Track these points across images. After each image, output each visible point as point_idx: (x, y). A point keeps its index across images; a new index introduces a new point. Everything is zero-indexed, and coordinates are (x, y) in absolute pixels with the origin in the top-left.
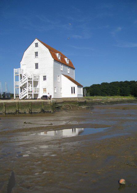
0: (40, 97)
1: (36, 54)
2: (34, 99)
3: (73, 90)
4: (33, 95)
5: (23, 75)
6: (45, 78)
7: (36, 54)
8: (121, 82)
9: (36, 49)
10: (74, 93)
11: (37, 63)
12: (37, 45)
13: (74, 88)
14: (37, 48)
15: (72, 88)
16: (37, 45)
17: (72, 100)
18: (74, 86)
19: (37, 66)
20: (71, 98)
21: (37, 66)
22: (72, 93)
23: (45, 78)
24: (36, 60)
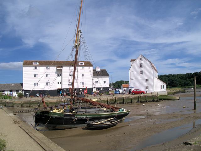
1: (141, 65)
3: (162, 87)
6: (147, 80)
7: (141, 65)
9: (141, 62)
12: (141, 59)
13: (163, 85)
15: (162, 85)
16: (141, 59)
18: (164, 84)
19: (141, 72)
21: (141, 72)
22: (162, 89)
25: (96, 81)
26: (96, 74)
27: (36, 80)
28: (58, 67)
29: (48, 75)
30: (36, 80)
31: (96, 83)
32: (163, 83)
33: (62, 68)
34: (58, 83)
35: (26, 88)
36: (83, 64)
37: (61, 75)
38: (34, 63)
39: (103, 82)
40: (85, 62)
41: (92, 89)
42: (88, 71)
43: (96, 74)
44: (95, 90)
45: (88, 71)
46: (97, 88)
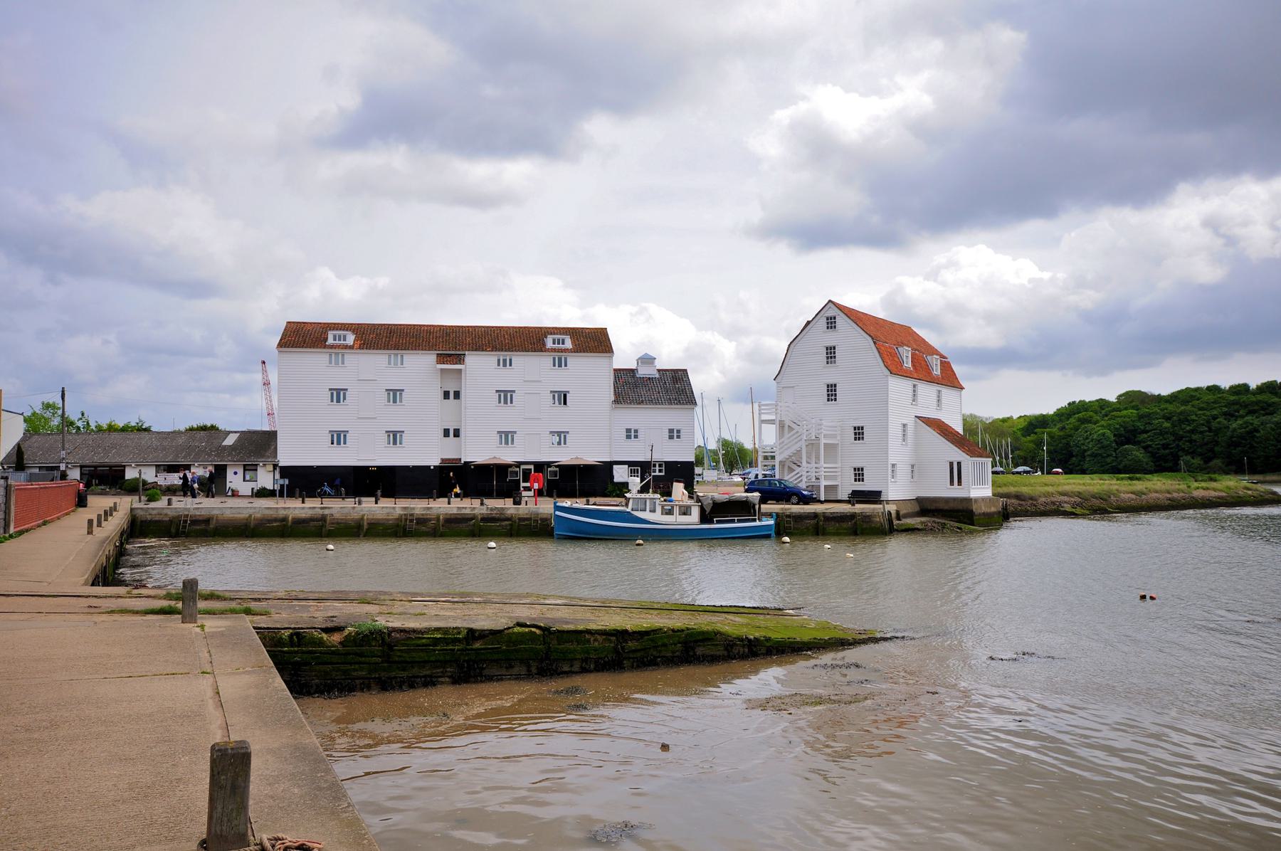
0: (844, 495)
1: (831, 353)
2: (826, 501)
3: (956, 474)
4: (822, 489)
5: (787, 423)
6: (859, 433)
7: (831, 353)
8: (1241, 389)
9: (831, 338)
10: (960, 483)
11: (831, 382)
13: (959, 464)
14: (831, 333)
15: (951, 464)
16: (831, 323)
17: (952, 505)
18: (959, 459)
19: (832, 391)
20: (947, 500)
21: (832, 391)
22: (952, 483)
23: (859, 433)
25: (628, 431)
27: (339, 417)
28: (442, 359)
29: (395, 395)
30: (339, 417)
31: (628, 437)
32: (956, 454)
33: (459, 359)
34: (446, 433)
35: (289, 455)
36: (569, 344)
37: (457, 395)
38: (330, 341)
40: (574, 333)
41: (608, 467)
44: (620, 474)
46: (630, 464)
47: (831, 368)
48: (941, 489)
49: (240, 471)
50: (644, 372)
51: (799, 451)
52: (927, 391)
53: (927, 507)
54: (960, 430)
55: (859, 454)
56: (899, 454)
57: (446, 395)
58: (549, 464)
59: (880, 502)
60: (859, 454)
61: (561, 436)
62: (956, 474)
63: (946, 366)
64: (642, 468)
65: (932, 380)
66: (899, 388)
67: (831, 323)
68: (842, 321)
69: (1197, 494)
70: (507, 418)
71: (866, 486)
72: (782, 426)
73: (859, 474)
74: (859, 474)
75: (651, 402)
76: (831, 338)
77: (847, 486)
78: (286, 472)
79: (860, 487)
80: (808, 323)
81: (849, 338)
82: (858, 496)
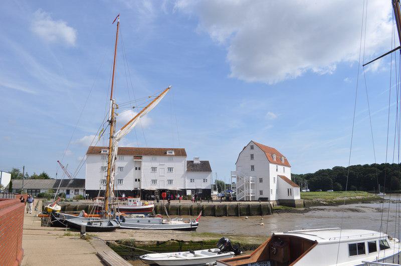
1: (252, 156)
6: (261, 180)
7: (252, 156)
8: (366, 166)
9: (252, 152)
14: (252, 151)
16: (252, 148)
19: (253, 167)
21: (253, 167)
23: (261, 180)
24: (253, 163)
26: (192, 167)
28: (136, 157)
31: (191, 181)
32: (290, 186)
33: (141, 158)
34: (136, 180)
35: (89, 186)
36: (173, 153)
37: (140, 169)
39: (200, 183)
40: (175, 150)
42: (180, 166)
43: (192, 167)
44: (189, 193)
45: (180, 166)
46: (192, 190)
47: (252, 161)
48: (285, 197)
49: (74, 191)
50: (196, 162)
51: (243, 186)
52: (280, 168)
53: (281, 202)
54: (290, 179)
55: (261, 186)
56: (273, 186)
57: (136, 169)
58: (167, 190)
59: (268, 201)
60: (261, 186)
61: (170, 182)
62: (290, 192)
63: (286, 160)
64: (194, 191)
65: (282, 165)
66: (272, 167)
67: (252, 148)
68: (255, 147)
69: (358, 197)
70: (154, 176)
71: (264, 196)
72: (238, 178)
73: (261, 193)
74: (261, 193)
75: (198, 171)
76: (252, 152)
77: (258, 196)
78: (88, 192)
79: (261, 196)
80: (245, 147)
81: (256, 152)
82: (262, 199)
